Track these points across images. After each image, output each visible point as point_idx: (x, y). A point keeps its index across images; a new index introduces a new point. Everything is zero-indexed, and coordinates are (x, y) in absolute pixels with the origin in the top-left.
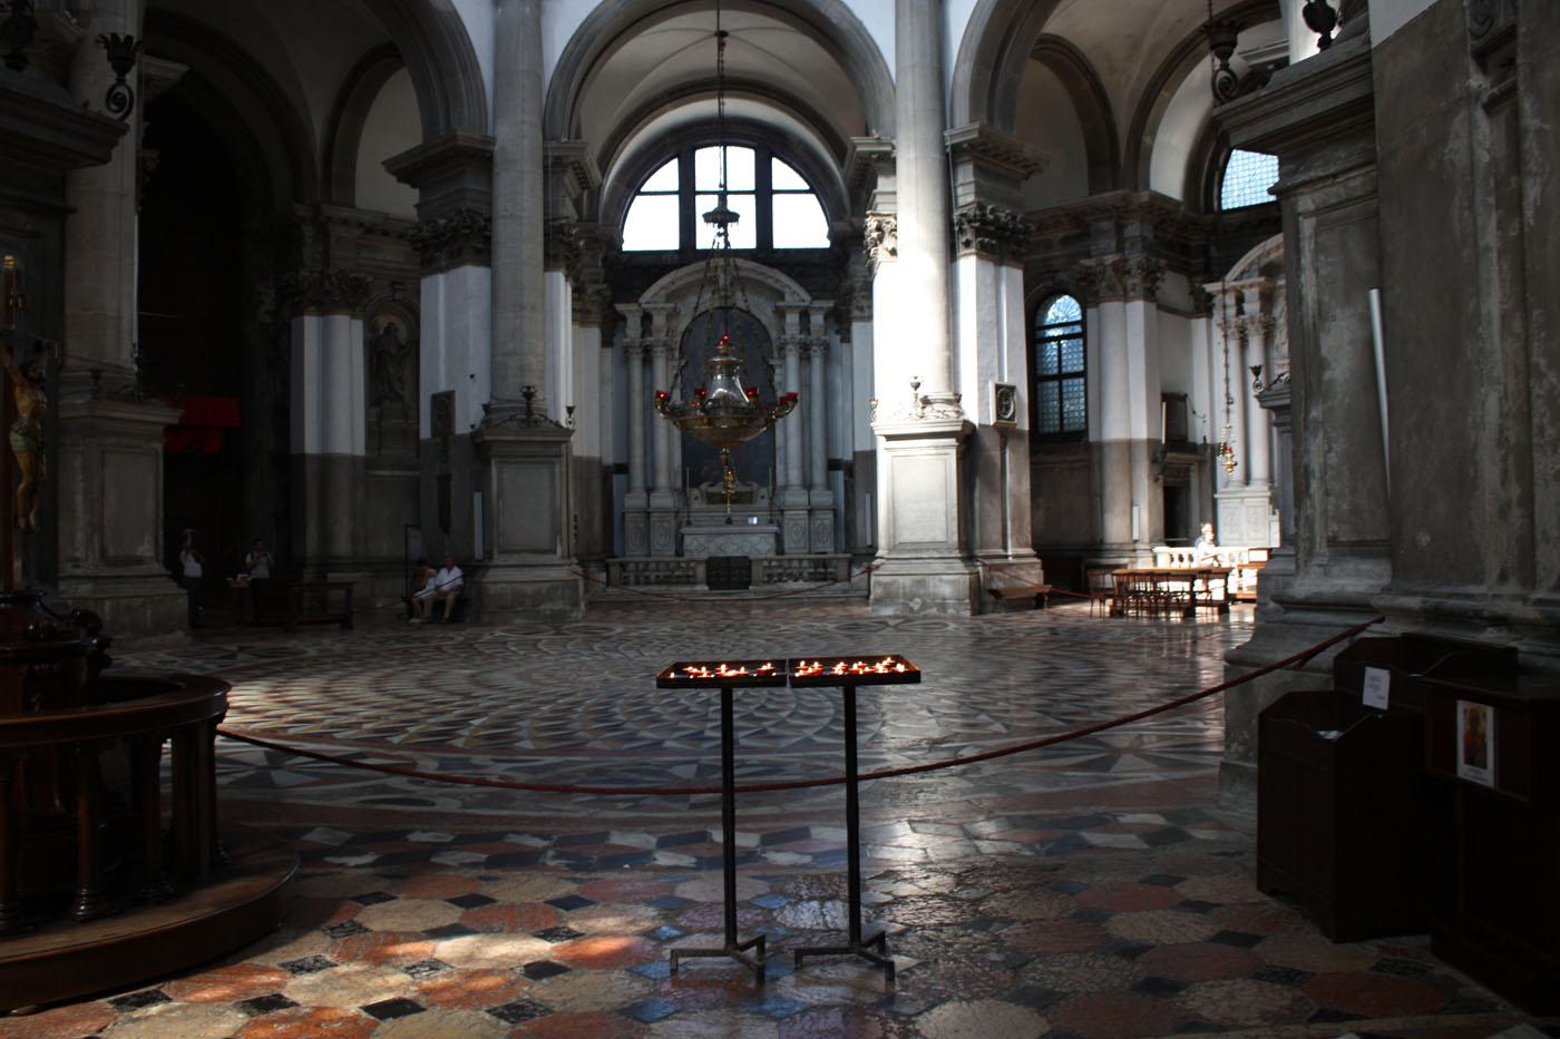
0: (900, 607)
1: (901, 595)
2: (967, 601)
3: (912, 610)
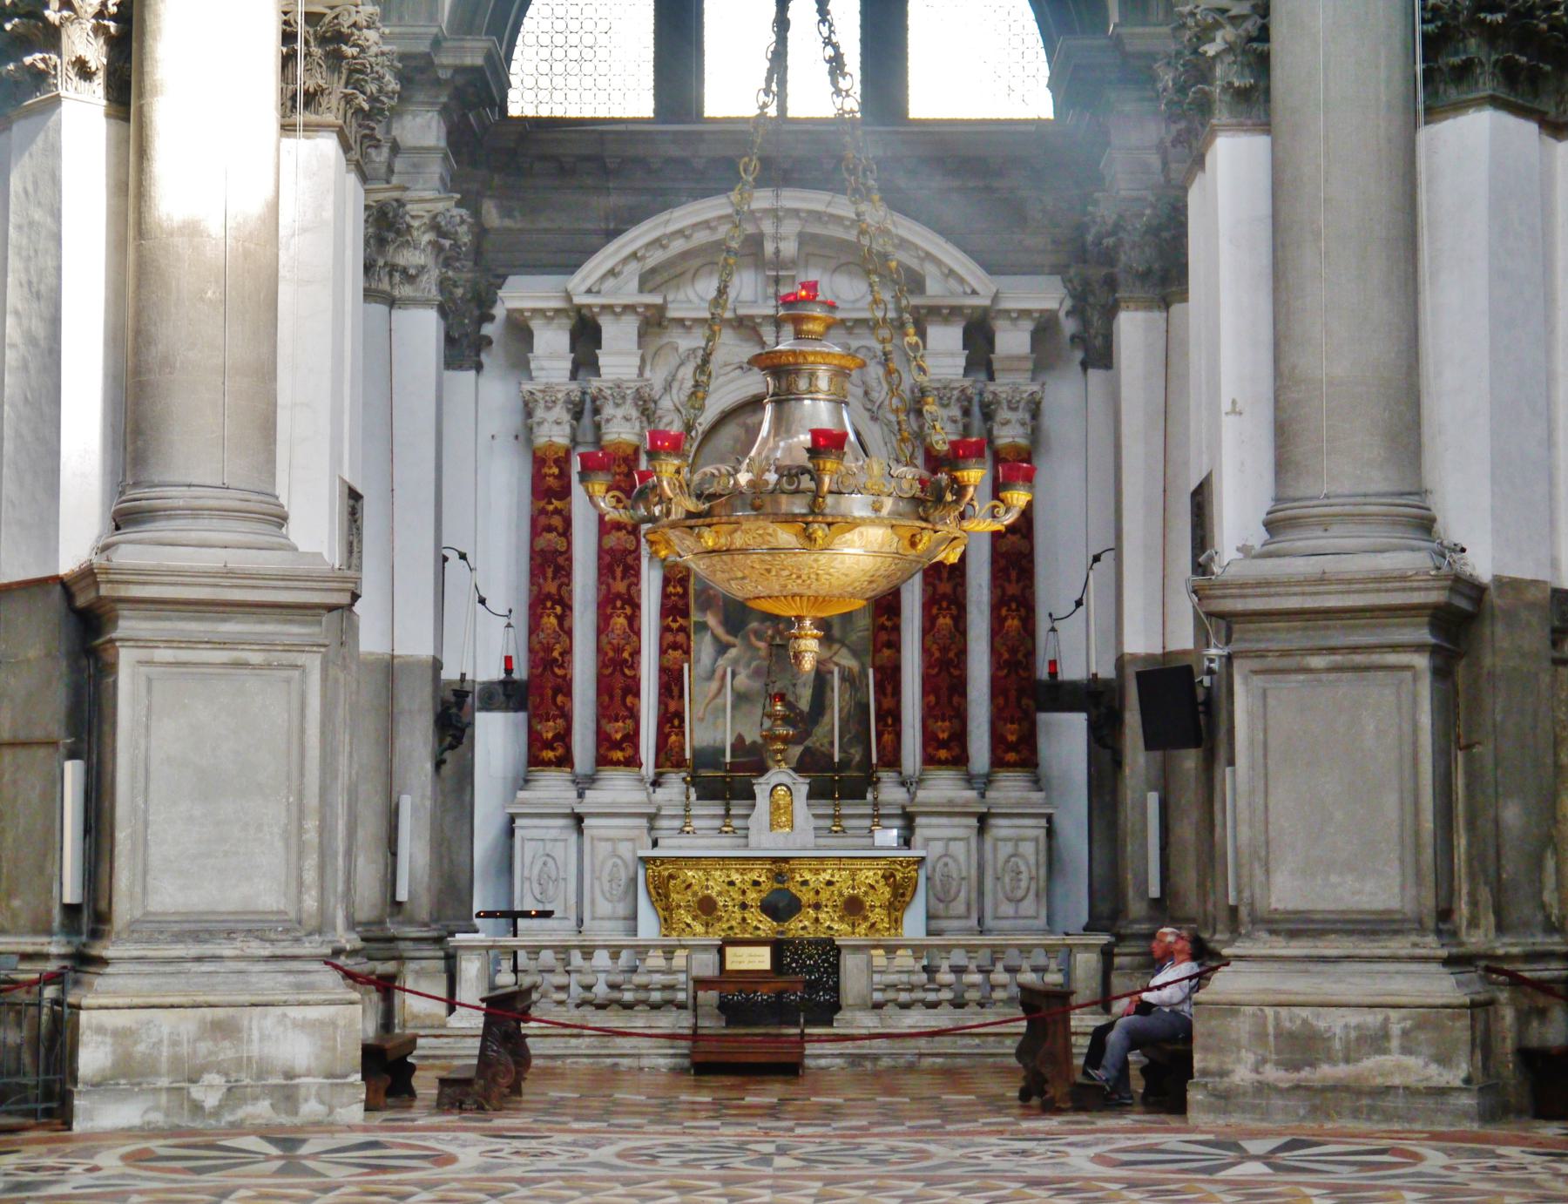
0: (164, 1098)
1: (164, 1066)
2: (358, 1076)
3: (197, 1108)
